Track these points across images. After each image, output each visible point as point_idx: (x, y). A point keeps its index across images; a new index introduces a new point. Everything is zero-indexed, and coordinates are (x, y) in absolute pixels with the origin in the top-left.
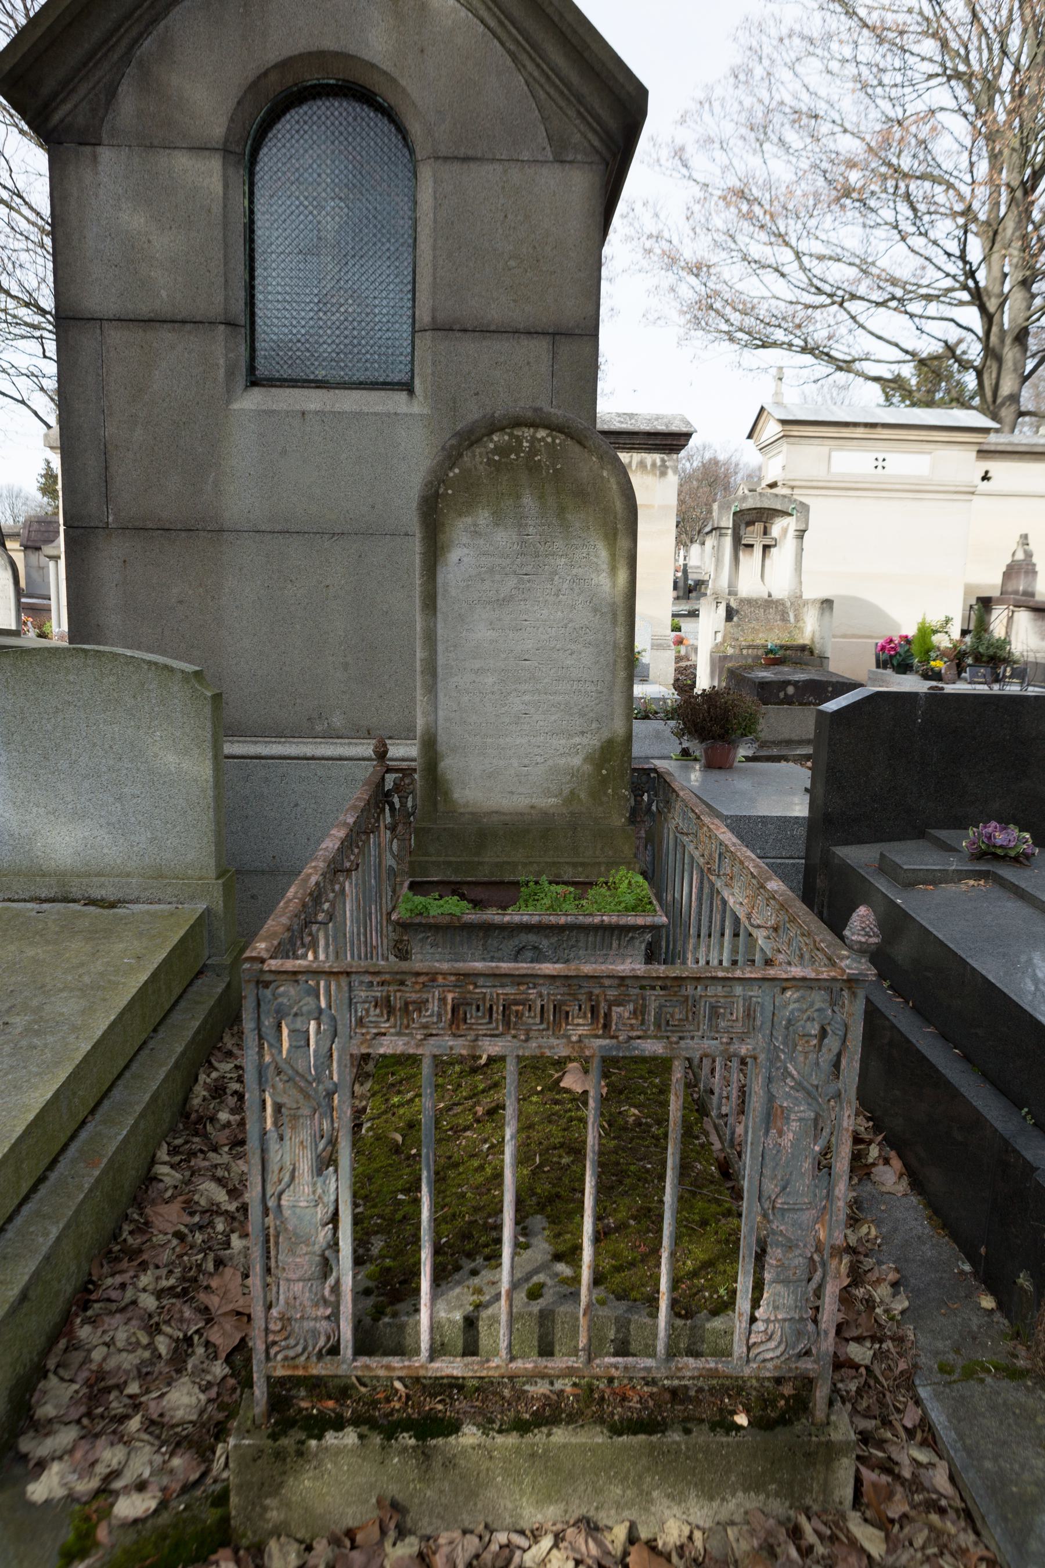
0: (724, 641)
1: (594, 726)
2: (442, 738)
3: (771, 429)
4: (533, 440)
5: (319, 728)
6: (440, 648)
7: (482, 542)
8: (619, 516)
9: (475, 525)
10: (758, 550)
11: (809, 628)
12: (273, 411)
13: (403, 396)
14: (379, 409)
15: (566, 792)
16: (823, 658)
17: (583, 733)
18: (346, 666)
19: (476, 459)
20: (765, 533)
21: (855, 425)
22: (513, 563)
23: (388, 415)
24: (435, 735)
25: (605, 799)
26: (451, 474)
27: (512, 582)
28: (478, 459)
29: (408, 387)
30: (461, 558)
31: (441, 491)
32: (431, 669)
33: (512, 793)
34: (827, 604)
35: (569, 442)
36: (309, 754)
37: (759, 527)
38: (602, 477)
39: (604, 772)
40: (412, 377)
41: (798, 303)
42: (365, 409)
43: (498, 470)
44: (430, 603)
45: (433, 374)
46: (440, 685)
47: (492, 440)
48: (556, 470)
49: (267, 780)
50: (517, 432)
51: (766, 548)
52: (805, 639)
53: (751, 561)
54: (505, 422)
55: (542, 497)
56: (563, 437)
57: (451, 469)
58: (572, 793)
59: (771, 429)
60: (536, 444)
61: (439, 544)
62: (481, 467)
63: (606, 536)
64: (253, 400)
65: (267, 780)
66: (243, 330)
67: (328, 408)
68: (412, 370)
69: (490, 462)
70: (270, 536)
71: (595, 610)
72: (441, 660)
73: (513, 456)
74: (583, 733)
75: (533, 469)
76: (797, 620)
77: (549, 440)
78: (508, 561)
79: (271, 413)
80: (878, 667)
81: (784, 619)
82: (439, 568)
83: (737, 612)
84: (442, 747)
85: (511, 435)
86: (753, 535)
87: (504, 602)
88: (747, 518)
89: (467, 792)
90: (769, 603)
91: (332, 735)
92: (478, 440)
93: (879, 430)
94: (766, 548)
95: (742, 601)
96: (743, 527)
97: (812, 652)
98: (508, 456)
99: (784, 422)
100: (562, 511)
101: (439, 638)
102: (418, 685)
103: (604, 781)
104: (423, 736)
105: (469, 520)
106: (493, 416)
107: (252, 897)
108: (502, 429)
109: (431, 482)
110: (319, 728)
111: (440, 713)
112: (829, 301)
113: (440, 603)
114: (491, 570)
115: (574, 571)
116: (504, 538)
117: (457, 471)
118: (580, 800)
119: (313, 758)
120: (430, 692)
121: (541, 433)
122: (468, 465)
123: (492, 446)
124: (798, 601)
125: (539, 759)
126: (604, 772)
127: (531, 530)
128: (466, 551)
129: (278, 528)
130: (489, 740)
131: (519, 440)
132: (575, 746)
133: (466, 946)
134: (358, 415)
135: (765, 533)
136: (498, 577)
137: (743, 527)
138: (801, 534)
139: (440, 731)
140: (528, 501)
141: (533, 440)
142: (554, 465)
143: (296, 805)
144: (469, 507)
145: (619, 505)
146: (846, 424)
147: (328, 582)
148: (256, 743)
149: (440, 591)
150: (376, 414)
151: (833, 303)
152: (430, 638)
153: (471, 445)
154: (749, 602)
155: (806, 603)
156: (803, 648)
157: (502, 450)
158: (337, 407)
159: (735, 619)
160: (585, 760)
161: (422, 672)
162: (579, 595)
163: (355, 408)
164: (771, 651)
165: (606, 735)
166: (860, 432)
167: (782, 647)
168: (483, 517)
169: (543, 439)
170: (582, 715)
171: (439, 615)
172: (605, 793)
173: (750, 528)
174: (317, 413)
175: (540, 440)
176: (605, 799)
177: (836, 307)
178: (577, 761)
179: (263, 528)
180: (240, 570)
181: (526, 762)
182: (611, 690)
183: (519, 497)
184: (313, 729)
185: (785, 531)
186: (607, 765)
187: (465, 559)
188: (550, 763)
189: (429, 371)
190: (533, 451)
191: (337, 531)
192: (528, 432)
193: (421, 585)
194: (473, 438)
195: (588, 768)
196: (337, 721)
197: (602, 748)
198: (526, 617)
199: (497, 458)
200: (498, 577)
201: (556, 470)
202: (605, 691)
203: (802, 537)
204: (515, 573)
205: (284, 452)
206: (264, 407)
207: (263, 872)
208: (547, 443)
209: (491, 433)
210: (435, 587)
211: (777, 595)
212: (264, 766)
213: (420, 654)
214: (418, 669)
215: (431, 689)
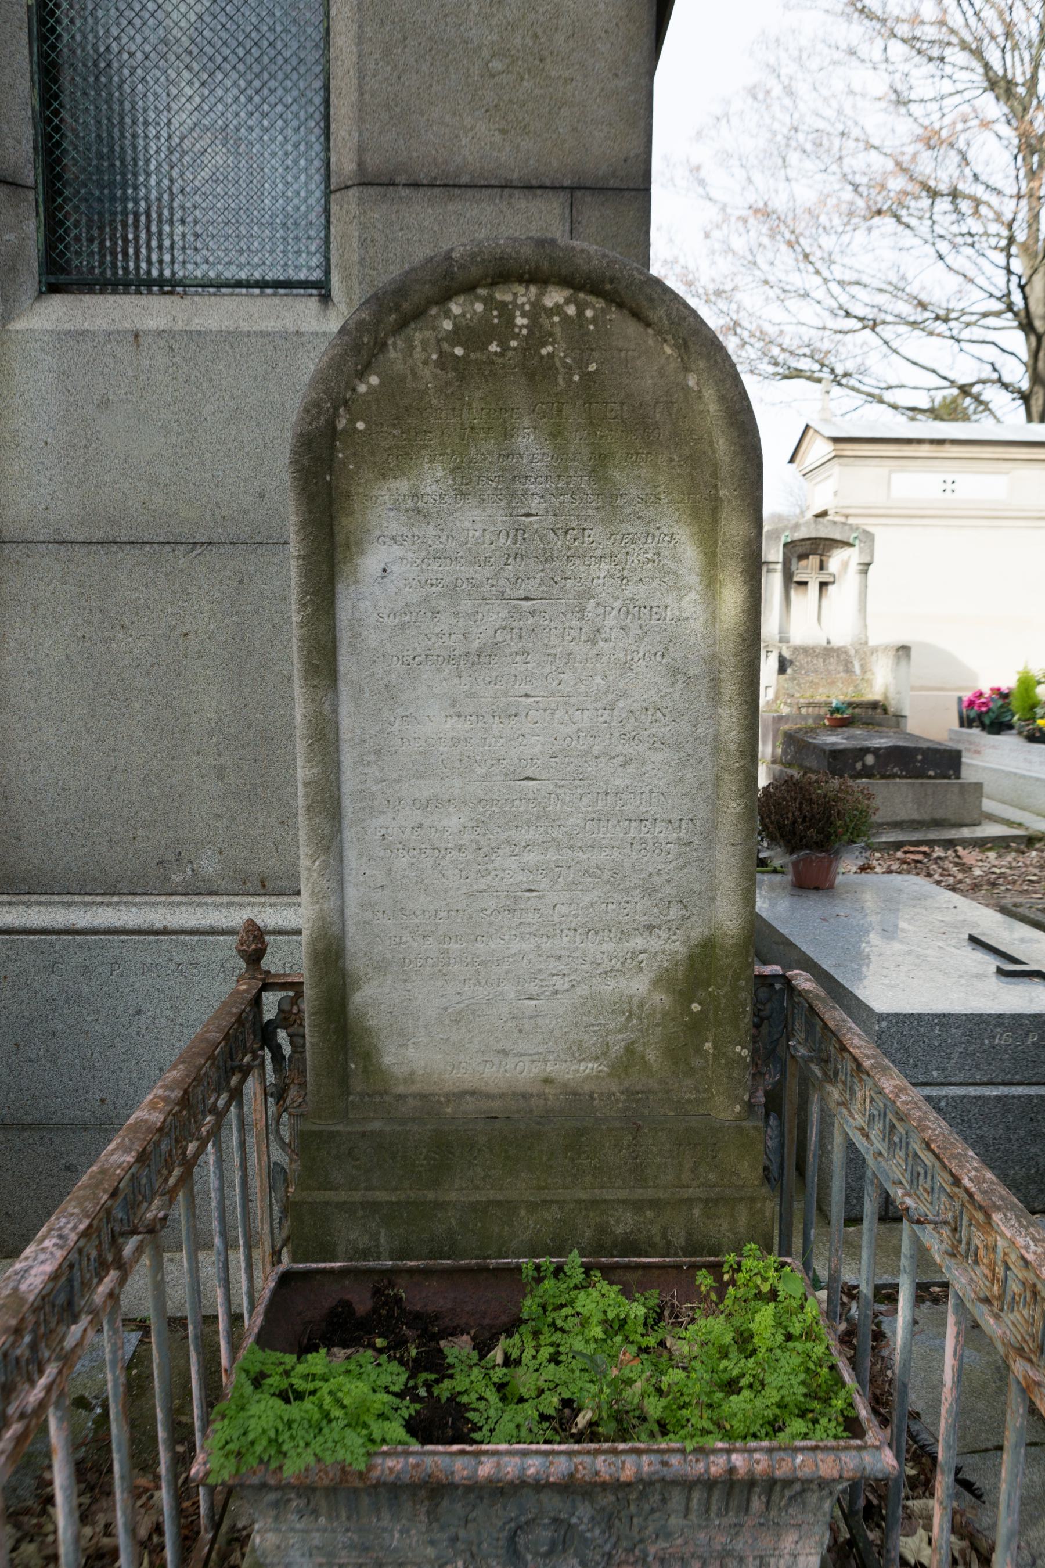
0: (777, 698)
1: (674, 912)
2: (356, 943)
3: (818, 450)
4: (537, 311)
5: (177, 878)
6: (348, 756)
7: (431, 531)
8: (724, 471)
9: (416, 496)
10: (813, 588)
11: (880, 682)
12: (84, 333)
13: (311, 305)
14: (270, 325)
15: (617, 1049)
16: (899, 717)
17: (650, 928)
18: (220, 772)
19: (414, 355)
20: (821, 568)
21: (920, 441)
22: (497, 575)
23: (285, 335)
24: (341, 938)
25: (697, 1062)
26: (362, 388)
27: (496, 614)
28: (418, 354)
29: (322, 289)
30: (391, 565)
31: (342, 423)
32: (328, 802)
33: (505, 1053)
34: (904, 651)
35: (614, 314)
36: (158, 926)
37: (814, 560)
38: (686, 389)
39: (696, 1007)
40: (327, 273)
41: (824, 328)
42: (245, 327)
43: (462, 378)
44: (323, 661)
45: (362, 262)
46: (349, 834)
47: (448, 314)
48: (586, 376)
49: (86, 970)
50: (503, 295)
51: (823, 585)
52: (875, 692)
53: (805, 601)
54: (475, 271)
55: (556, 434)
56: (600, 304)
57: (361, 375)
58: (629, 1049)
59: (818, 450)
60: (544, 320)
61: (340, 538)
62: (426, 372)
63: (695, 515)
64: (56, 314)
65: (86, 970)
66: (31, 195)
67: (180, 326)
68: (327, 259)
69: (445, 361)
70: (84, 550)
71: (674, 672)
72: (349, 782)
73: (494, 348)
74: (650, 928)
75: (538, 373)
76: (864, 671)
77: (571, 310)
78: (488, 571)
79: (81, 334)
80: (962, 725)
81: (849, 670)
82: (340, 587)
83: (791, 662)
84: (356, 962)
85: (489, 302)
86: (806, 571)
87: (482, 656)
88: (800, 550)
89: (411, 1052)
90: (829, 652)
91: (198, 889)
92: (418, 314)
93: (947, 447)
94: (823, 585)
95: (796, 649)
96: (794, 561)
97: (885, 710)
98: (484, 348)
99: (836, 440)
100: (599, 464)
101: (345, 735)
102: (302, 835)
103: (696, 1027)
104: (313, 942)
105: (402, 486)
106: (448, 256)
107: (68, 1168)
108: (469, 288)
109: (317, 404)
110: (177, 878)
111: (352, 893)
112: (859, 325)
113: (345, 662)
114: (452, 591)
115: (630, 590)
116: (477, 521)
117: (374, 380)
118: (645, 1064)
119: (165, 931)
120: (327, 849)
121: (555, 297)
122: (399, 367)
123: (448, 325)
124: (864, 650)
125: (561, 984)
126: (696, 1007)
127: (535, 504)
128: (397, 551)
129: (99, 535)
130: (454, 946)
131: (506, 312)
132: (635, 954)
133: (386, 1515)
134: (231, 337)
135: (821, 568)
136: (466, 606)
137: (794, 561)
138: (865, 568)
139: (351, 929)
140: (529, 443)
141: (537, 311)
142: (581, 363)
143: (139, 1012)
144: (402, 457)
145: (722, 447)
146: (909, 441)
147: (187, 627)
148: (69, 905)
149: (344, 636)
150: (263, 334)
151: (864, 327)
152: (325, 738)
153: (402, 325)
154: (805, 650)
155: (874, 651)
156: (874, 705)
157: (471, 335)
158: (196, 325)
159: (789, 671)
160: (656, 982)
161: (308, 809)
162: (639, 639)
163: (228, 324)
164: (837, 710)
165: (698, 931)
166: (925, 450)
167: (850, 704)
168: (432, 478)
169: (558, 309)
170: (649, 891)
171: (344, 688)
172: (699, 1051)
173: (803, 563)
174: (160, 333)
175: (550, 312)
176: (697, 1062)
177: (867, 331)
178: (638, 986)
179: (73, 536)
180: (35, 608)
181: (533, 989)
182: (709, 838)
183: (507, 434)
184: (167, 879)
185: (845, 565)
186: (701, 993)
187: (396, 569)
188: (583, 990)
189: (355, 257)
190: (537, 336)
191: (199, 539)
192: (524, 295)
193: (302, 625)
194: (406, 306)
195: (661, 999)
196: (209, 865)
197: (691, 957)
198: (527, 688)
199: (459, 351)
200: (466, 606)
201: (586, 376)
202: (697, 841)
203: (865, 572)
204: (502, 596)
205: (104, 404)
206: (68, 326)
207: (85, 1127)
208: (566, 318)
209: (445, 297)
210: (332, 629)
211: (836, 642)
212: (80, 946)
213: (303, 771)
214: (301, 802)
215: (330, 844)
